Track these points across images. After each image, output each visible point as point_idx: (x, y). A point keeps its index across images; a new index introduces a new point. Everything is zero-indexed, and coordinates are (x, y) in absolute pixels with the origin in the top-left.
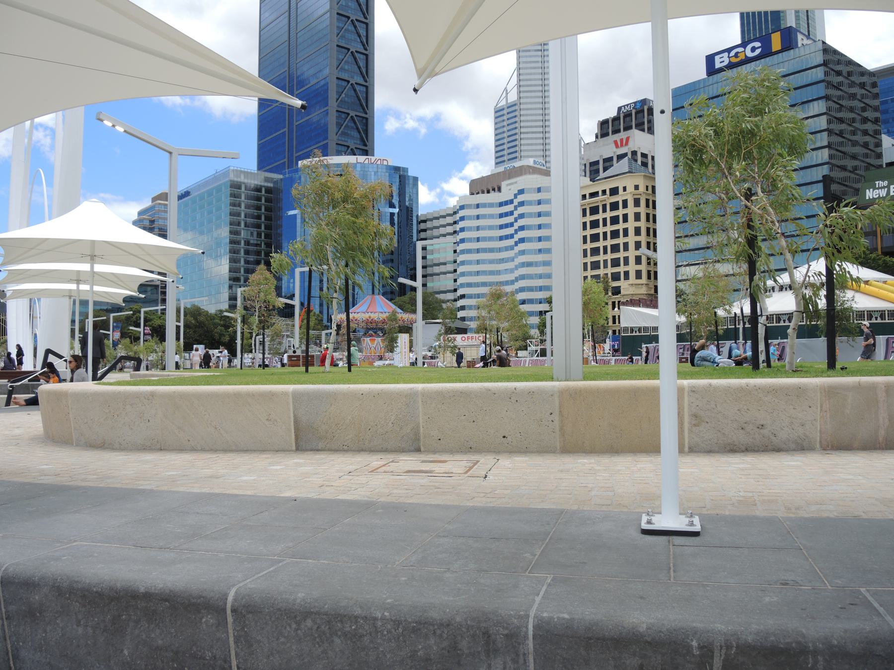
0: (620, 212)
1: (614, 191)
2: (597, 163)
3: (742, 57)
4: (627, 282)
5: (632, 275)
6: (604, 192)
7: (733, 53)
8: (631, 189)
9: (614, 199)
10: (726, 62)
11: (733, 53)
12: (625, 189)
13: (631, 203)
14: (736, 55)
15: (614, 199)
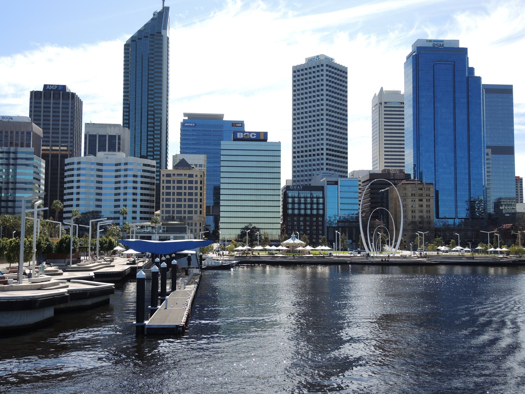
0: (194, 185)
1: (191, 176)
2: (95, 136)
3: (248, 137)
4: (196, 215)
5: (199, 212)
6: (185, 175)
7: (245, 134)
8: (199, 176)
9: (191, 179)
10: (242, 137)
11: (245, 134)
12: (196, 176)
13: (199, 182)
14: (246, 135)
15: (191, 179)
